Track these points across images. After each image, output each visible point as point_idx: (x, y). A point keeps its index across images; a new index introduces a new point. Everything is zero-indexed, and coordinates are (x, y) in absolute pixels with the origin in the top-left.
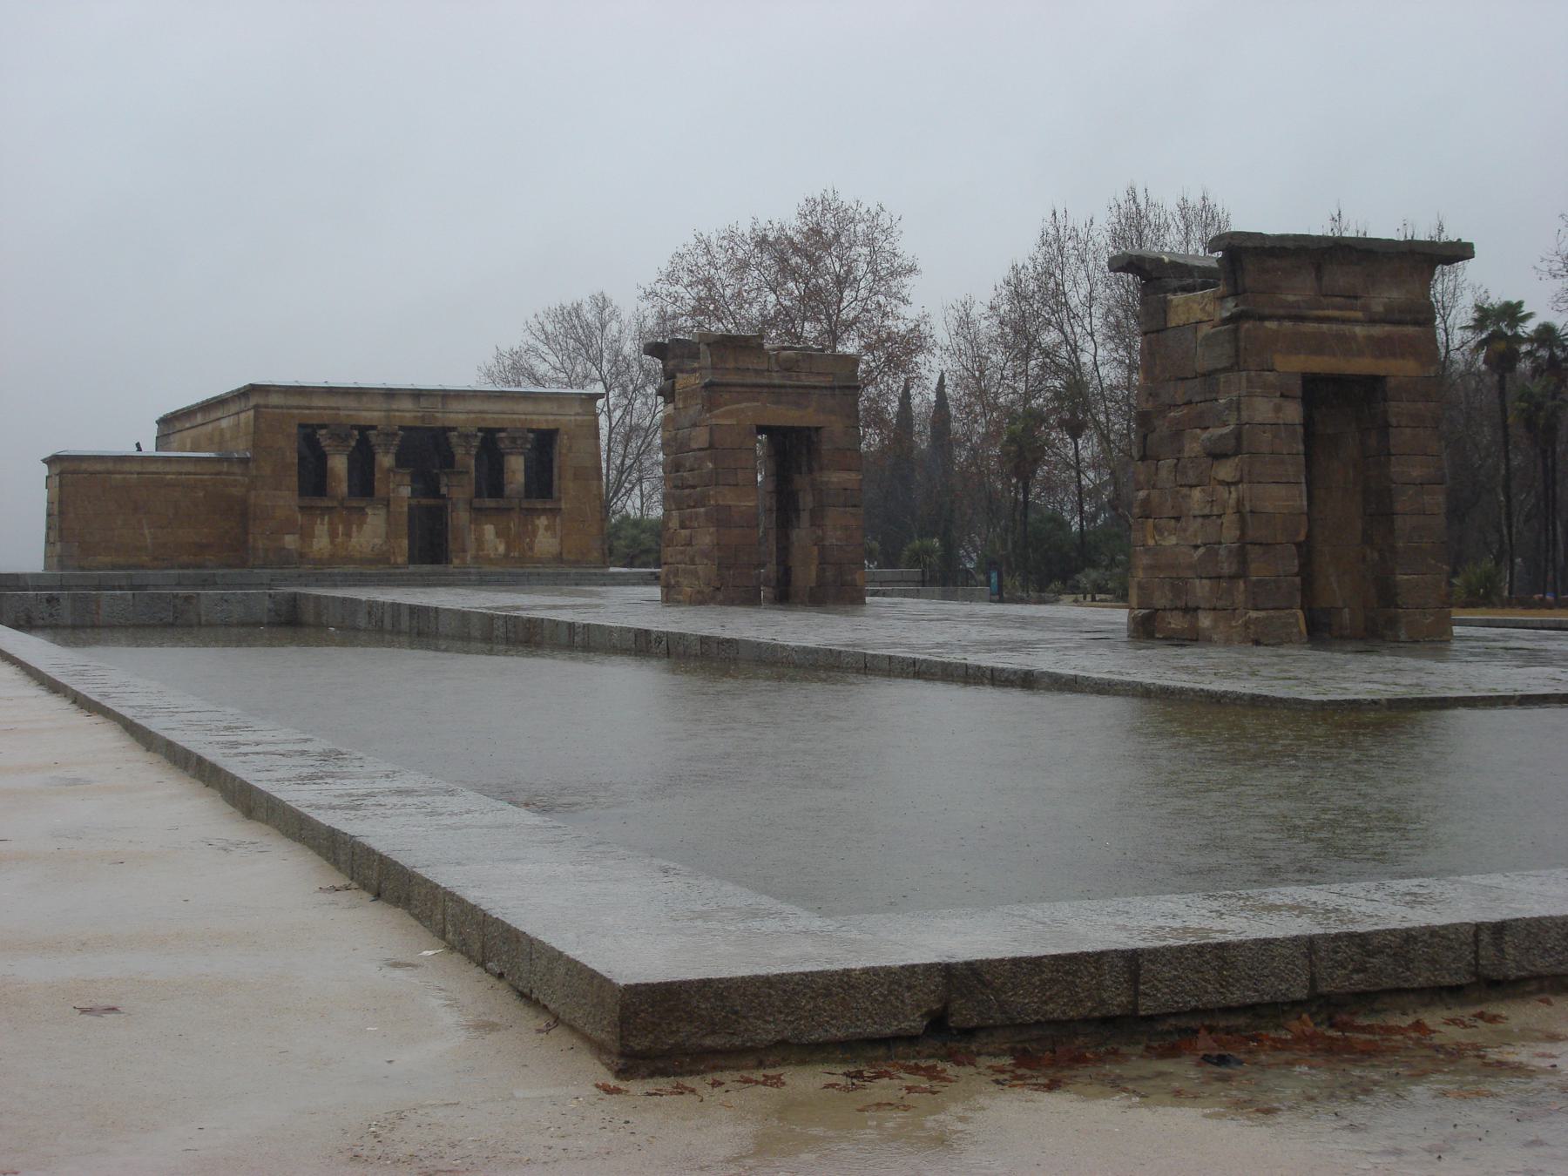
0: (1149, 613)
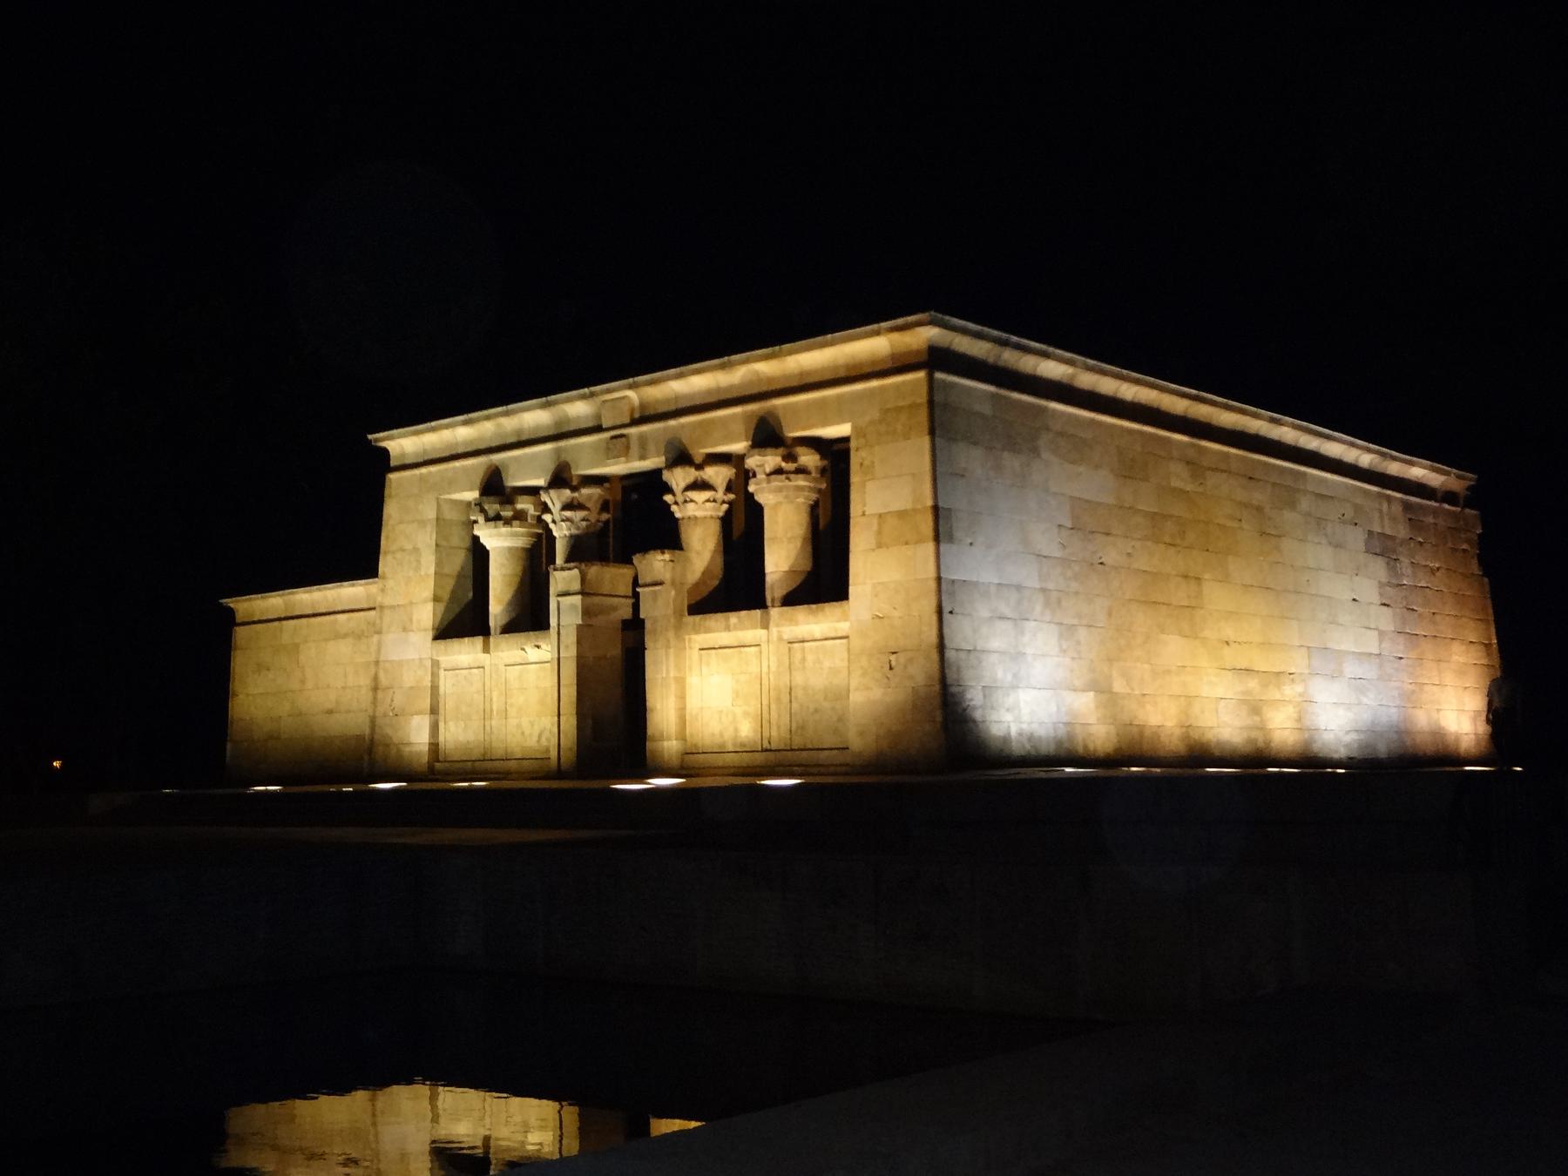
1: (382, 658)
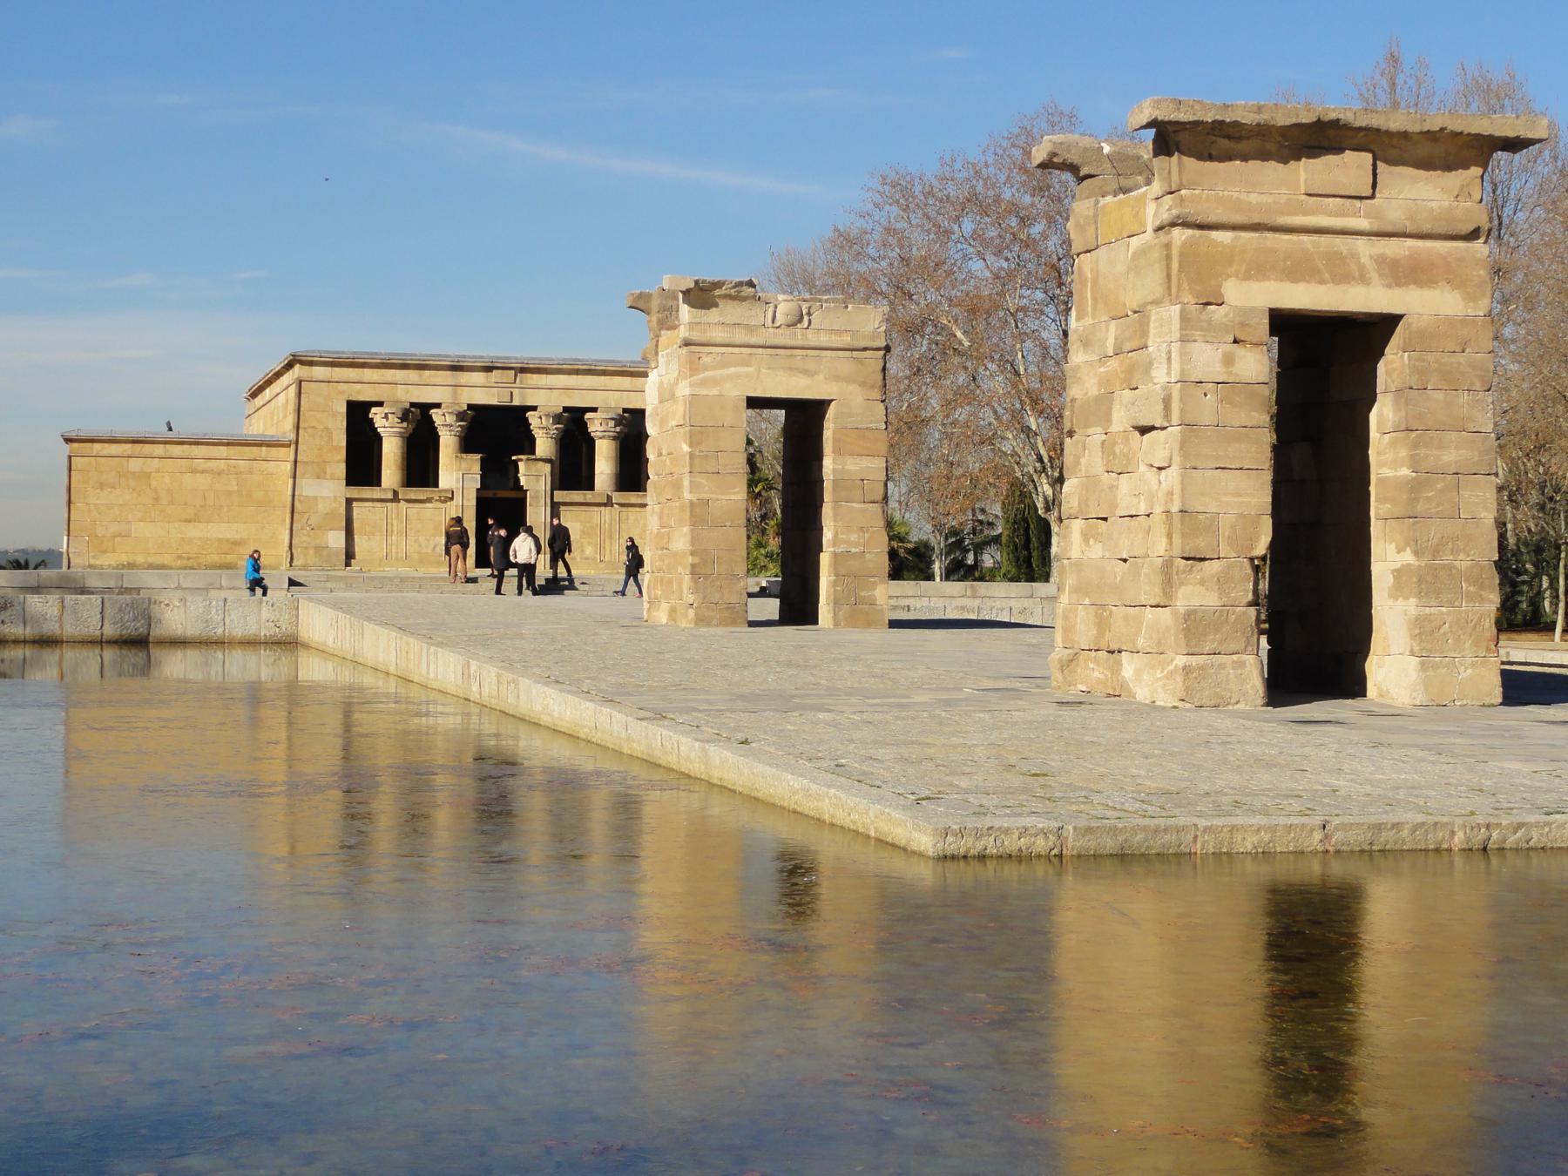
0: (1069, 655)
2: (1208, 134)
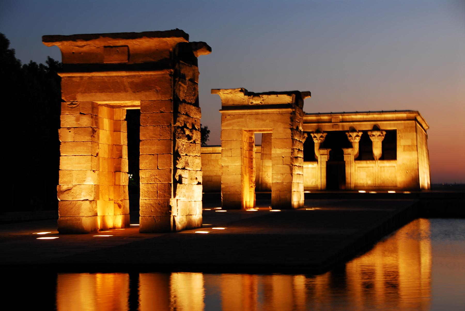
1: (263, 165)
2: (70, 46)
